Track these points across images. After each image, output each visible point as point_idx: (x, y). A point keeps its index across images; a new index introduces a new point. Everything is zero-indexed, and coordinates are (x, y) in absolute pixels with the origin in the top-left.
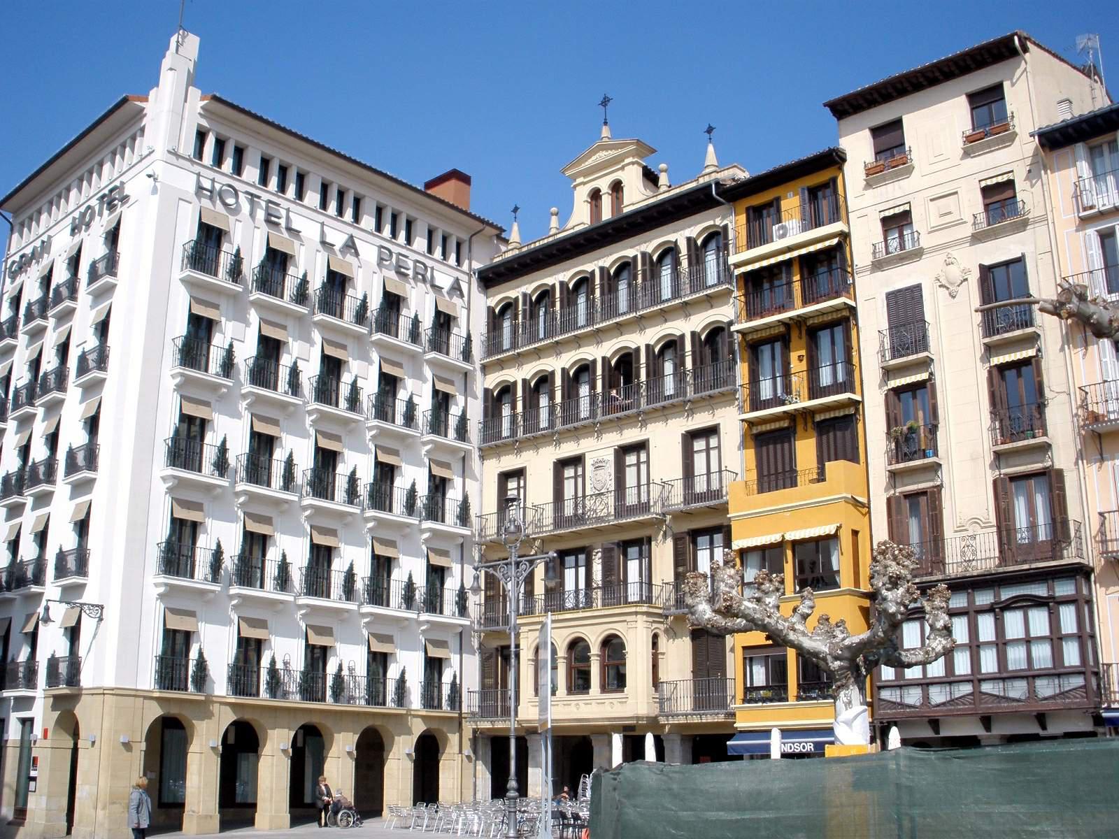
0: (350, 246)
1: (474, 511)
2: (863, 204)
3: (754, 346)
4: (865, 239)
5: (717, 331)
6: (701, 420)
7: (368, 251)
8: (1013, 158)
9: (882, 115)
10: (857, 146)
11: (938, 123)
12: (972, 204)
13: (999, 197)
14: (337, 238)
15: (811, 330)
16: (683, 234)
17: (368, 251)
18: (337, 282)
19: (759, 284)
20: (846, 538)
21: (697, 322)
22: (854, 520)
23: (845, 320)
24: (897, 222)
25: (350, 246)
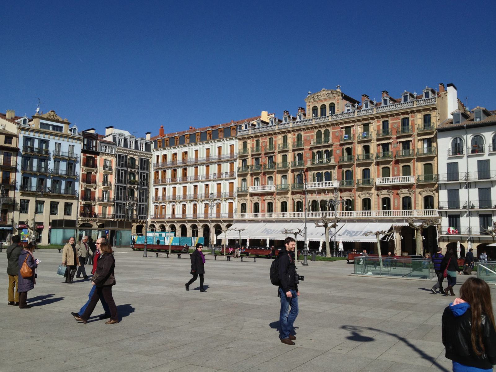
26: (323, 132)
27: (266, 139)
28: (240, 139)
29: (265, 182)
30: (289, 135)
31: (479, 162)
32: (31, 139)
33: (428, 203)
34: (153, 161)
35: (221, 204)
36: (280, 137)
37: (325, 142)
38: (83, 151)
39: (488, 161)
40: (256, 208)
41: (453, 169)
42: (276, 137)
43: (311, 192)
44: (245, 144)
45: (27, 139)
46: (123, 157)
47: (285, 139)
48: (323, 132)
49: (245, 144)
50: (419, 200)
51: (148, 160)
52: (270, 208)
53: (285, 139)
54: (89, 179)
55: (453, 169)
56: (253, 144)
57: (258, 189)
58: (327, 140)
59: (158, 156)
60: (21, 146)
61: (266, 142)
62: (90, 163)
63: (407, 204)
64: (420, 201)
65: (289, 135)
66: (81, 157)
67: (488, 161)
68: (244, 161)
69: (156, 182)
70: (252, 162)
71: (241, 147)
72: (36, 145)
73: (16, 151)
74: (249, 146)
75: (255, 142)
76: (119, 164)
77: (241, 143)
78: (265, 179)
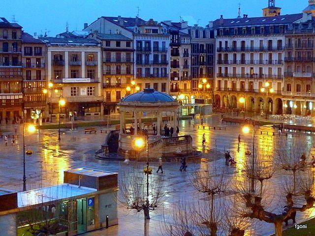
29: (305, 70)
32: (140, 42)
34: (217, 46)
38: (171, 45)
45: (139, 42)
46: (196, 45)
51: (212, 45)
54: (175, 65)
56: (296, 41)
57: (300, 75)
59: (221, 43)
60: (135, 48)
62: (175, 53)
66: (169, 49)
69: (220, 62)
70: (296, 54)
71: (287, 43)
72: (143, 46)
73: (133, 51)
74: (293, 42)
75: (297, 40)
76: (193, 51)
77: (287, 39)
78: (305, 67)
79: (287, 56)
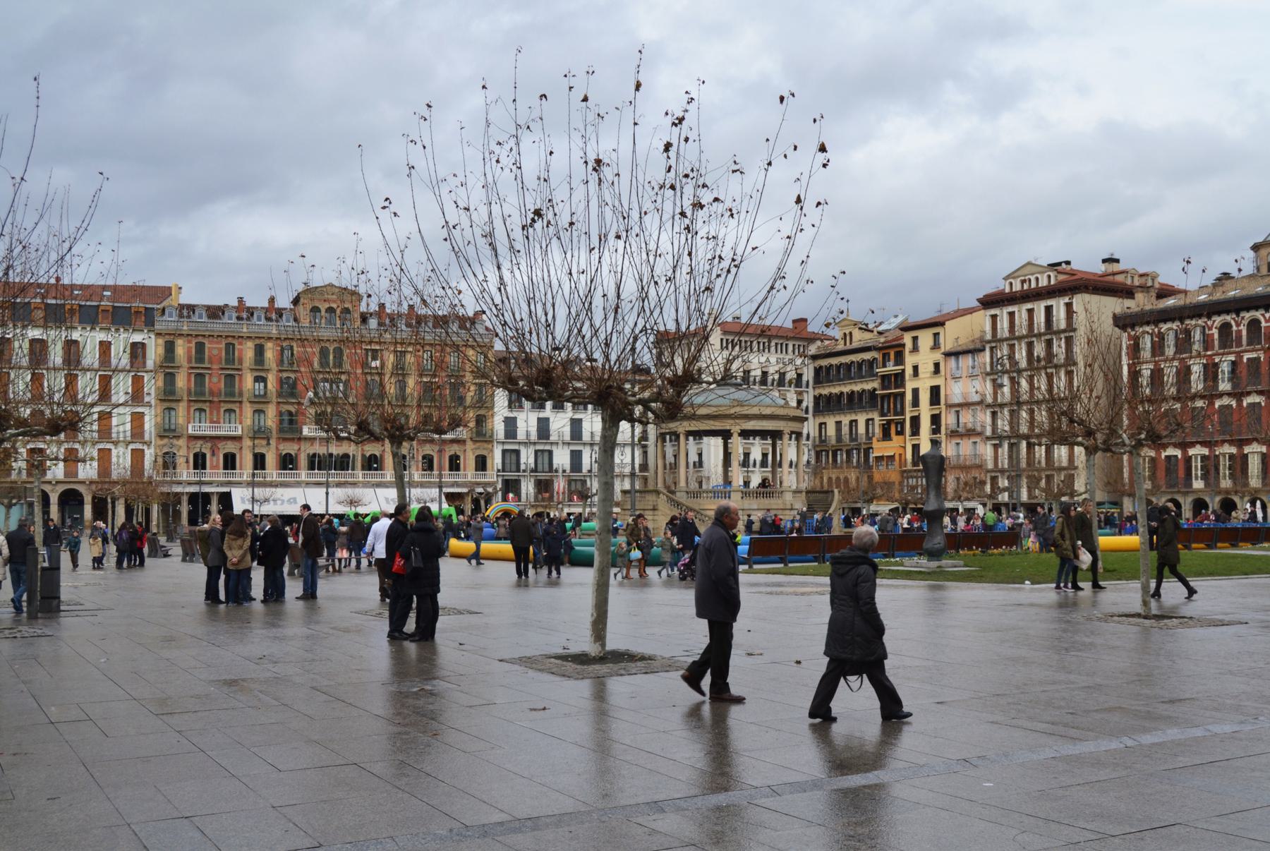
0: (768, 360)
1: (812, 435)
2: (910, 360)
3: (883, 397)
4: (909, 371)
5: (875, 389)
6: (870, 416)
7: (773, 360)
8: (938, 356)
9: (914, 333)
10: (907, 339)
11: (925, 338)
12: (932, 368)
13: (937, 365)
14: (763, 359)
15: (895, 395)
16: (867, 356)
17: (773, 360)
18: (765, 374)
19: (885, 379)
20: (897, 457)
21: (868, 386)
22: (901, 451)
23: (903, 395)
24: (916, 368)
25: (768, 360)
26: (331, 349)
27: (220, 343)
28: (158, 335)
30: (269, 345)
31: (539, 419)
33: (481, 464)
35: (114, 452)
36: (250, 345)
37: (335, 366)
39: (547, 420)
40: (199, 462)
41: (510, 424)
42: (240, 344)
43: (312, 439)
44: (170, 348)
47: (260, 350)
48: (331, 349)
49: (170, 348)
50: (469, 461)
52: (230, 462)
53: (260, 350)
55: (510, 424)
56: (189, 349)
57: (206, 429)
58: (339, 364)
61: (220, 350)
63: (454, 464)
64: (471, 463)
65: (269, 345)
67: (547, 420)
68: (170, 378)
70: (189, 380)
71: (161, 350)
75: (193, 345)
77: (161, 341)
79: (161, 383)
